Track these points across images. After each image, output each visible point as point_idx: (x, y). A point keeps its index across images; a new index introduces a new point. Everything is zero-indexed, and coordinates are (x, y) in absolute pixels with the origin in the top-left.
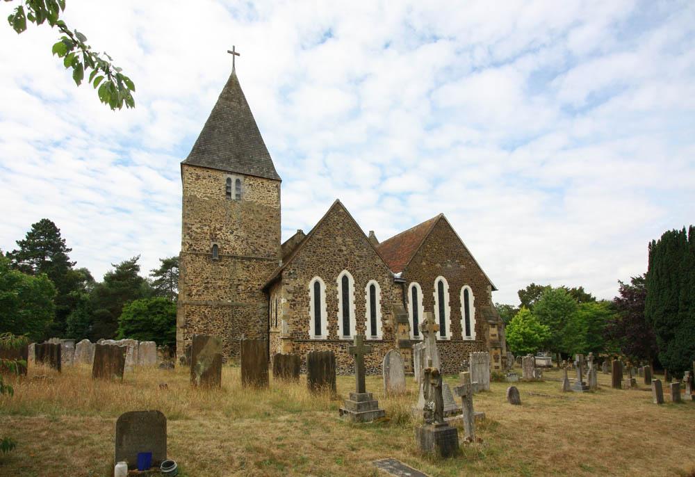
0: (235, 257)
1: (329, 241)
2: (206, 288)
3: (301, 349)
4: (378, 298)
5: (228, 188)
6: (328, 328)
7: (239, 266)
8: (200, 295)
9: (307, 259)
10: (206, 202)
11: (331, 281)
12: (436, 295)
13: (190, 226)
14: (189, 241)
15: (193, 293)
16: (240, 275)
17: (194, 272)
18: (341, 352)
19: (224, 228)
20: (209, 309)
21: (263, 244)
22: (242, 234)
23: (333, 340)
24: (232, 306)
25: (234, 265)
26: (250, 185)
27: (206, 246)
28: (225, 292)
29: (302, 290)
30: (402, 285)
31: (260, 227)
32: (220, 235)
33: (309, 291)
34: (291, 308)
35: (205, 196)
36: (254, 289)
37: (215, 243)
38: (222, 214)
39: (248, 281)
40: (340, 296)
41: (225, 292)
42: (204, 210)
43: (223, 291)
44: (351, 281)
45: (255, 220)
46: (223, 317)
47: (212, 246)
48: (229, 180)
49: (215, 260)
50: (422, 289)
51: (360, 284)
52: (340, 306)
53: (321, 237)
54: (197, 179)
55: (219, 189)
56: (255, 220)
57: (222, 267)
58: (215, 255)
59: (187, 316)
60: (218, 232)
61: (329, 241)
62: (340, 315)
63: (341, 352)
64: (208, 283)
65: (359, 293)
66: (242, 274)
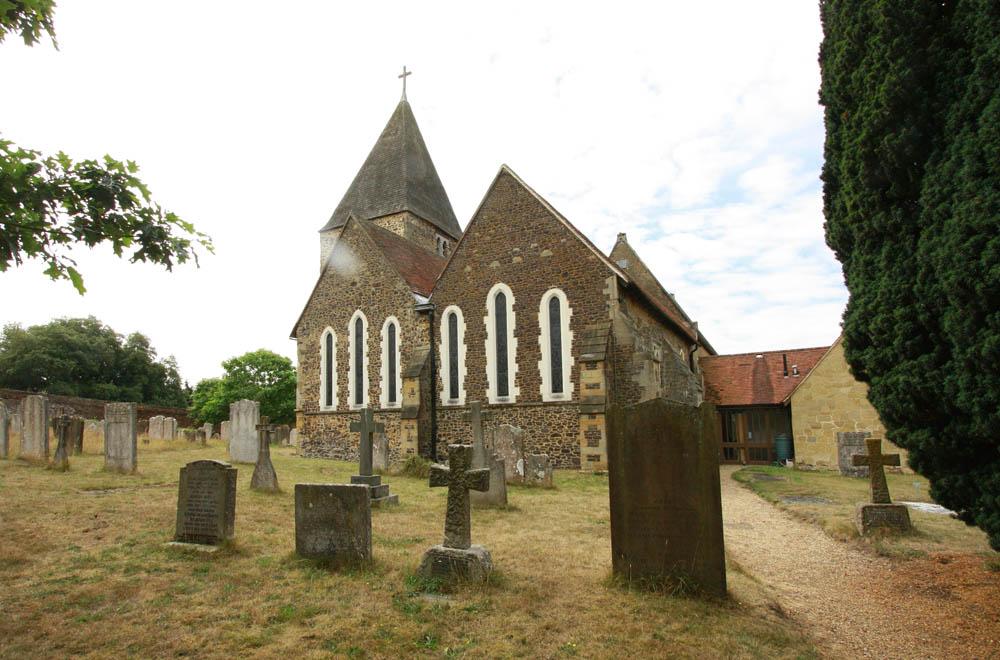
4: (398, 342)
6: (338, 396)
23: (343, 412)
30: (430, 315)
33: (320, 347)
40: (352, 350)
51: (375, 326)
65: (373, 339)
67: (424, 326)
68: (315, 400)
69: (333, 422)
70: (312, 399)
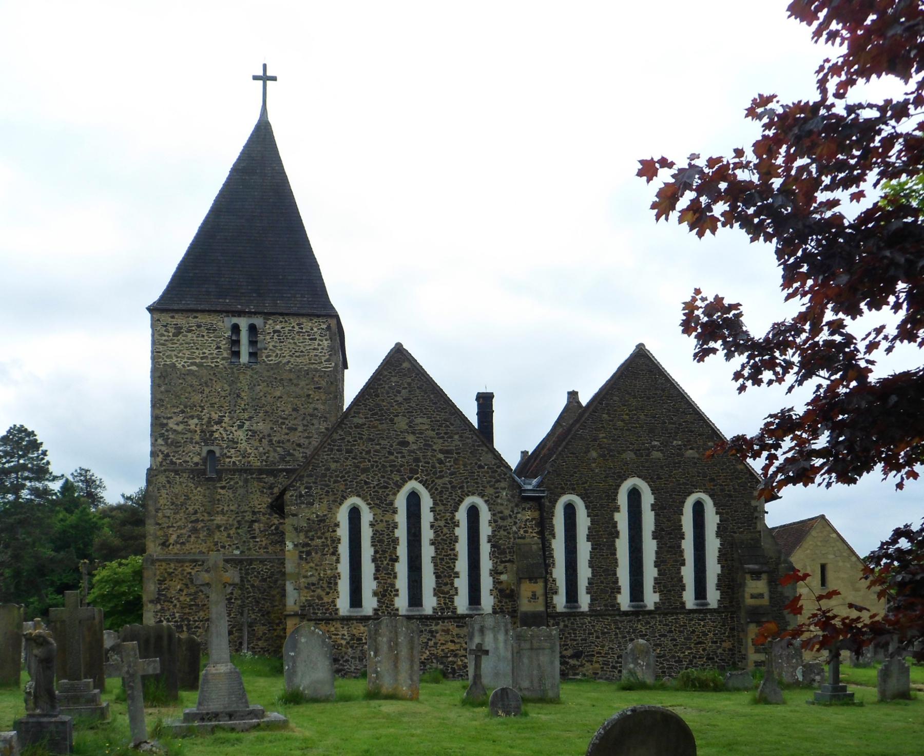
0: (246, 471)
2: (195, 530)
5: (237, 342)
8: (183, 543)
10: (191, 373)
11: (383, 505)
12: (622, 519)
13: (165, 421)
14: (163, 448)
16: (256, 503)
17: (173, 503)
19: (226, 419)
21: (302, 441)
24: (241, 562)
26: (275, 332)
27: (194, 455)
28: (229, 536)
31: (295, 410)
32: (219, 431)
35: (193, 364)
37: (212, 448)
38: (223, 394)
41: (229, 536)
42: (189, 389)
44: (427, 502)
47: (204, 454)
48: (236, 329)
49: (210, 479)
50: (587, 507)
52: (402, 551)
57: (222, 491)
59: (161, 582)
64: (197, 521)
68: (326, 600)
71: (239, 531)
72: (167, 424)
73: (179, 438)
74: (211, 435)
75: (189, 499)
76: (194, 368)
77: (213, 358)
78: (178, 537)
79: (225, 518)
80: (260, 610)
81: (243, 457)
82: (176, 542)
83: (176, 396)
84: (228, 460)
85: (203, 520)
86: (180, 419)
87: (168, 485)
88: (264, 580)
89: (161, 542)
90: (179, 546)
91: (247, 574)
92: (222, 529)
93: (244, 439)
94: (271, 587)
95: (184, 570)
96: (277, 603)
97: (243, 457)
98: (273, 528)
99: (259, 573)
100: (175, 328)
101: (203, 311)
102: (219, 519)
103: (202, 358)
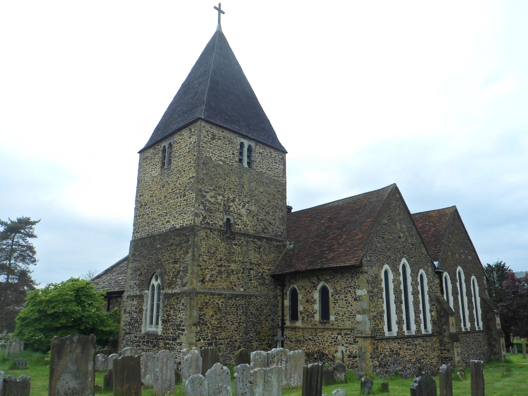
1: (393, 226)
2: (220, 272)
3: (379, 349)
7: (251, 246)
8: (213, 281)
9: (379, 245)
13: (205, 194)
14: (203, 212)
15: (207, 279)
18: (407, 349)
19: (237, 200)
20: (223, 300)
22: (253, 208)
23: (400, 337)
24: (246, 296)
25: (247, 246)
29: (376, 279)
33: (382, 281)
34: (370, 300)
35: (221, 160)
36: (264, 274)
37: (229, 217)
39: (259, 265)
43: (236, 276)
45: (264, 192)
46: (237, 310)
47: (225, 220)
53: (386, 222)
54: (213, 139)
55: (233, 154)
56: (264, 192)
57: (235, 247)
58: (228, 232)
59: (201, 309)
60: (231, 204)
61: (393, 226)
62: (403, 306)
63: (407, 349)
64: (221, 266)
65: (414, 283)
66: (254, 256)
67: (437, 281)
69: (394, 345)
70: (378, 326)
71: (244, 275)
72: (205, 196)
73: (212, 207)
74: (229, 209)
75: (218, 250)
76: (221, 163)
77: (231, 160)
78: (211, 276)
79: (236, 266)
80: (255, 331)
81: (245, 226)
82: (210, 280)
83: (211, 179)
84: (237, 226)
85: (225, 266)
86: (213, 194)
87: (206, 239)
88: (257, 310)
89: (201, 279)
90: (211, 283)
91: (249, 305)
92: (235, 273)
93: (245, 214)
94: (260, 315)
95: (214, 301)
96: (263, 326)
97: (245, 226)
98: (260, 274)
99: (255, 305)
100: (212, 135)
101: (227, 129)
102: (233, 266)
103: (225, 158)
